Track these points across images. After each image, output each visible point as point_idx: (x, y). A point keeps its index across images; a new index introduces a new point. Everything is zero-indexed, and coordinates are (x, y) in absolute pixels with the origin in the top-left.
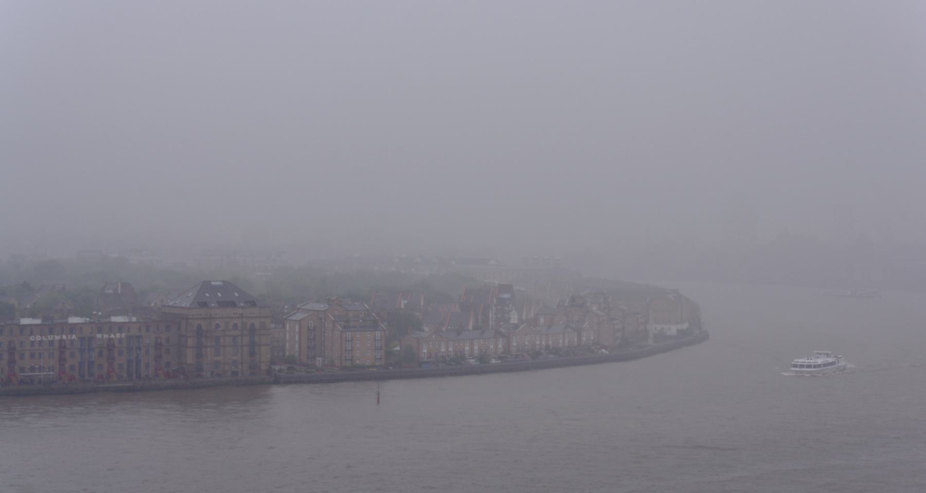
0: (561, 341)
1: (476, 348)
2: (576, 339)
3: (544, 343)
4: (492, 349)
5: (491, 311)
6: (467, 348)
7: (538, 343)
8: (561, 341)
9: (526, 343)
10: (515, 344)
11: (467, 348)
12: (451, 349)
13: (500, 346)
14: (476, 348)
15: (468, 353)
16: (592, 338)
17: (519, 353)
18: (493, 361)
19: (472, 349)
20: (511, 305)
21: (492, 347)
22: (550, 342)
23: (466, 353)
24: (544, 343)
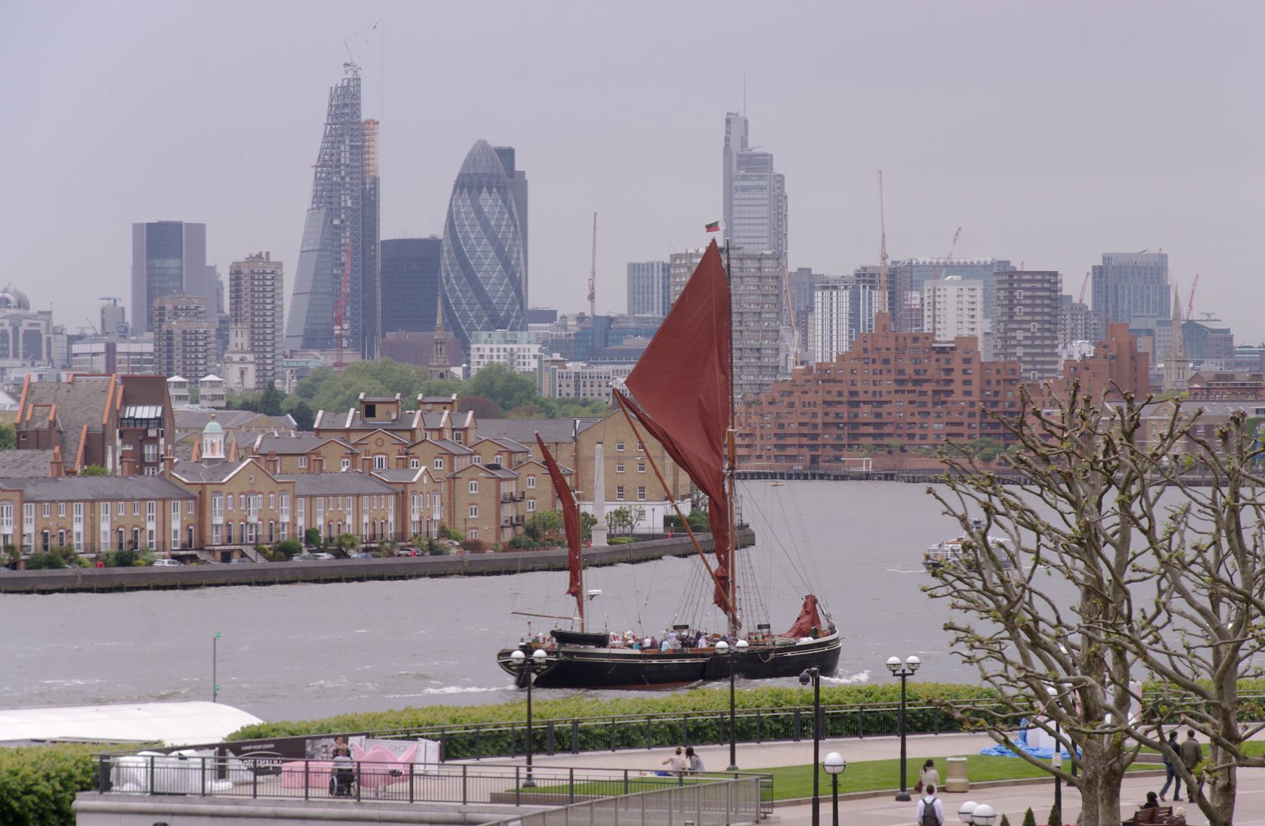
0: (349, 520)
1: (105, 527)
2: (391, 518)
3: (301, 522)
4: (151, 532)
5: (110, 449)
6: (78, 528)
7: (285, 518)
8: (349, 520)
9: (253, 519)
10: (219, 520)
11: (78, 528)
12: (29, 529)
13: (176, 525)
14: (105, 527)
15: (82, 541)
16: (437, 516)
17: (233, 547)
18: (164, 564)
19: (93, 528)
20: (162, 441)
21: (151, 526)
22: (320, 522)
23: (75, 542)
24: (301, 522)
